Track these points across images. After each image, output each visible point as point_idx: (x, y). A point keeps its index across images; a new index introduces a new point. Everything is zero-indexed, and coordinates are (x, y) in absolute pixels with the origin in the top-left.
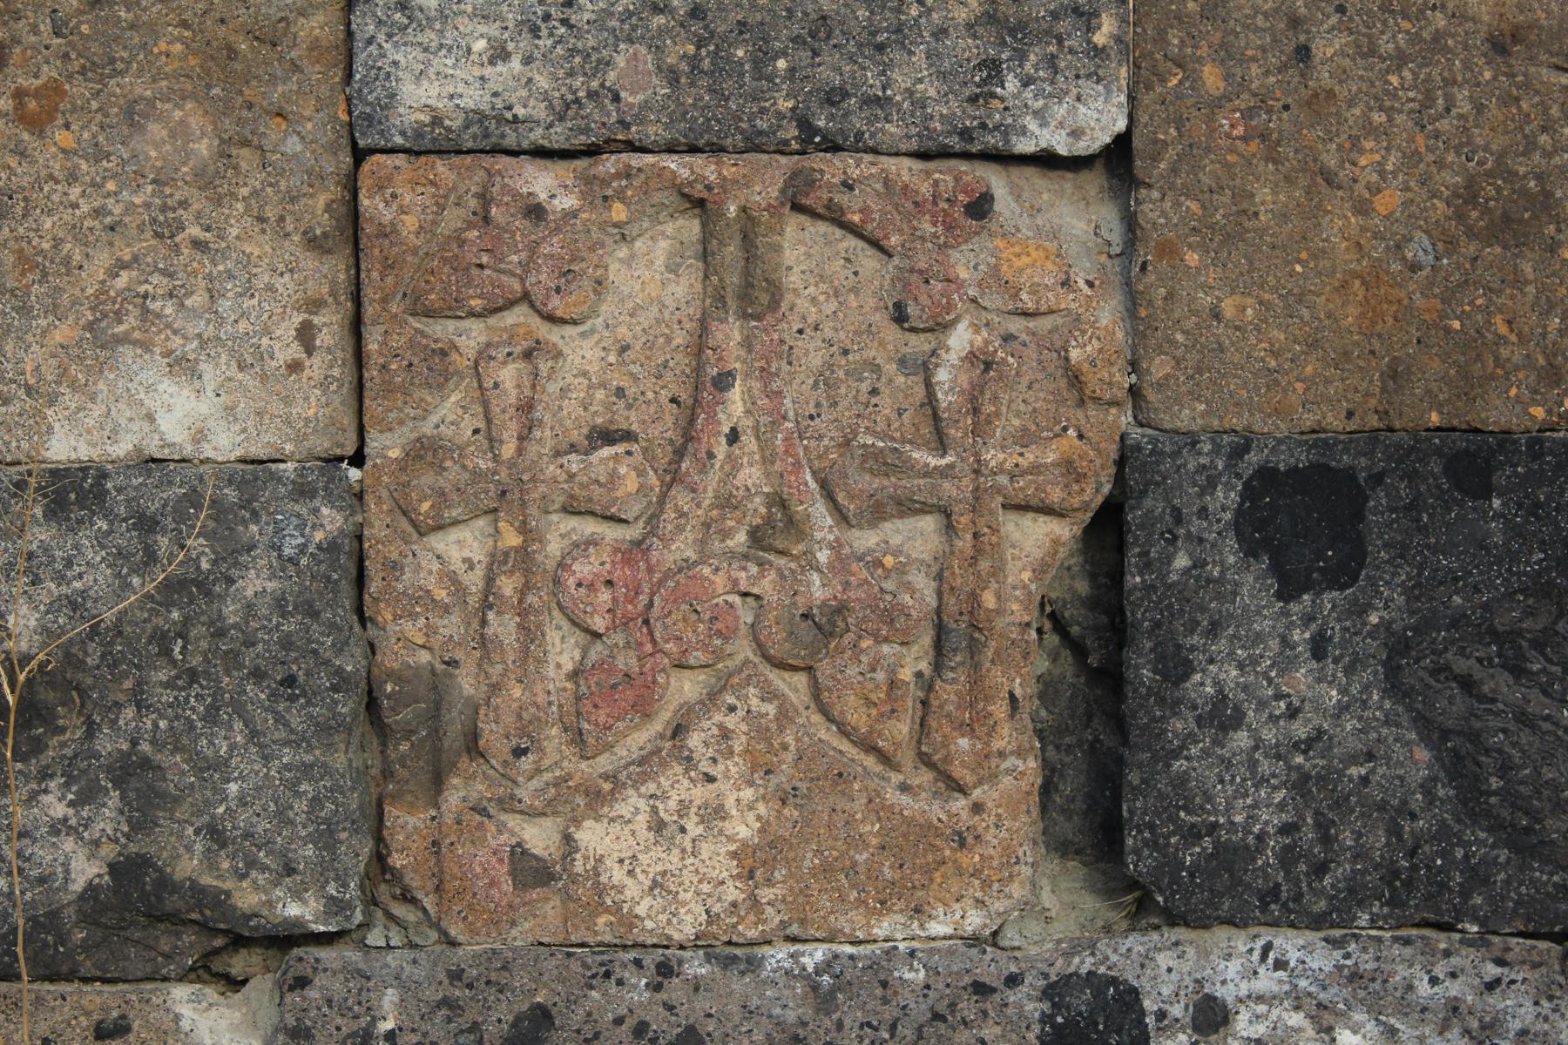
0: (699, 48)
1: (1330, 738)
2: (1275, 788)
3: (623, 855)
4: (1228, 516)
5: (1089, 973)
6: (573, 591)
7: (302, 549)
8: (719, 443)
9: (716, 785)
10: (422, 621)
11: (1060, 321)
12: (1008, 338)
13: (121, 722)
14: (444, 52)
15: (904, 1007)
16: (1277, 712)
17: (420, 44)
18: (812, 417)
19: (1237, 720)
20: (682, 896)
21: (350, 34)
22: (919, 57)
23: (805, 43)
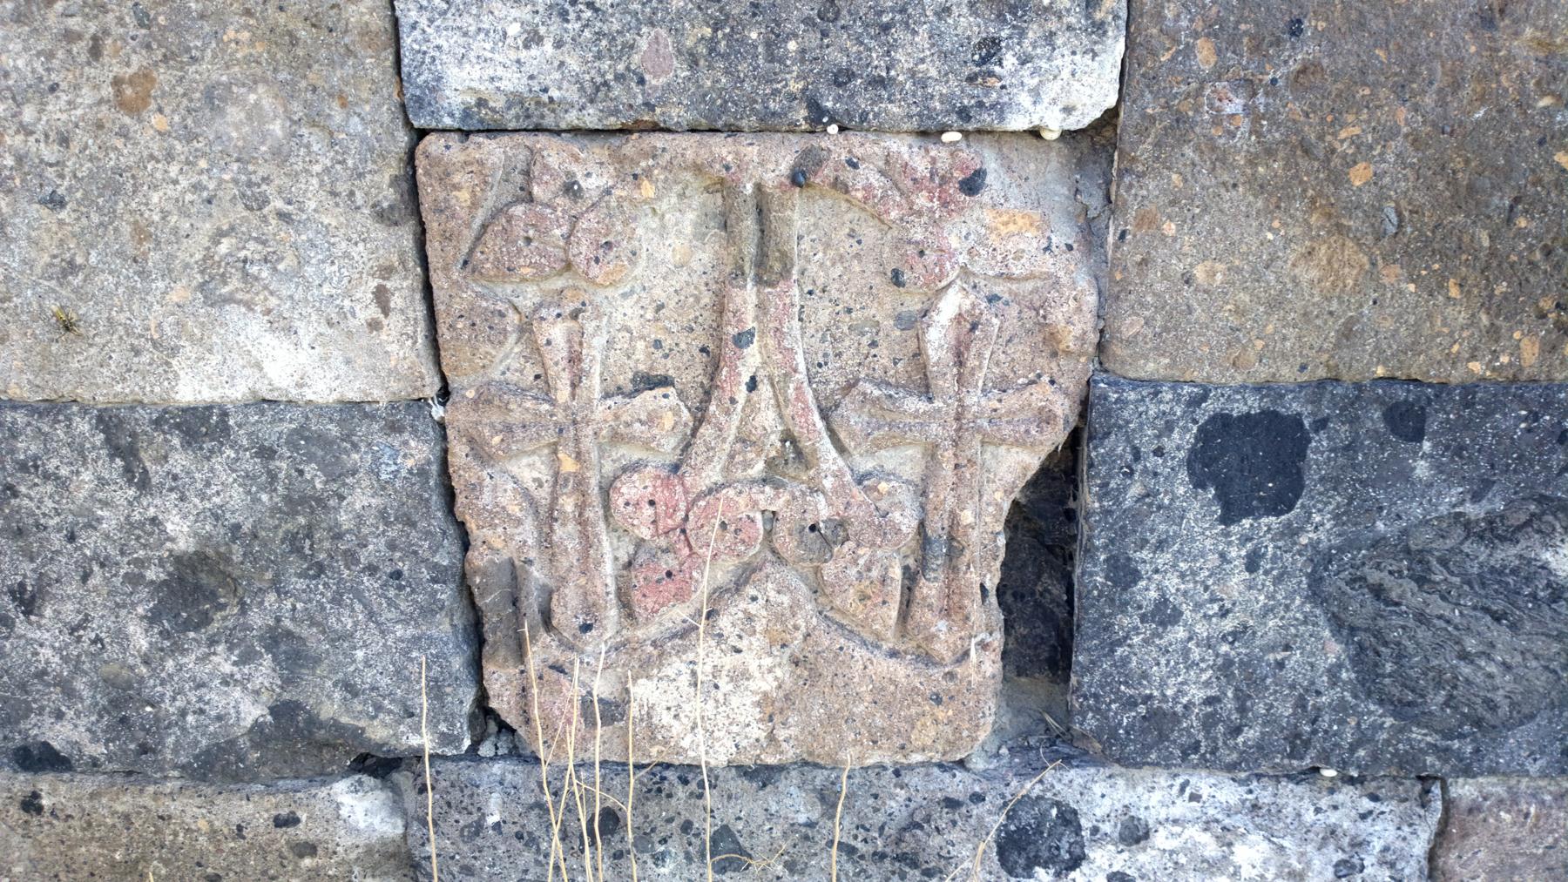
0: (715, 31)
1: (1254, 633)
2: (1203, 670)
4: (1182, 454)
6: (622, 509)
7: (396, 473)
10: (500, 530)
11: (1040, 284)
12: (992, 299)
13: (266, 604)
14: (482, 36)
15: (890, 815)
16: (1211, 613)
17: (460, 28)
18: (820, 365)
19: (1175, 617)
20: (716, 734)
21: (396, 22)
22: (922, 38)
23: (815, 25)
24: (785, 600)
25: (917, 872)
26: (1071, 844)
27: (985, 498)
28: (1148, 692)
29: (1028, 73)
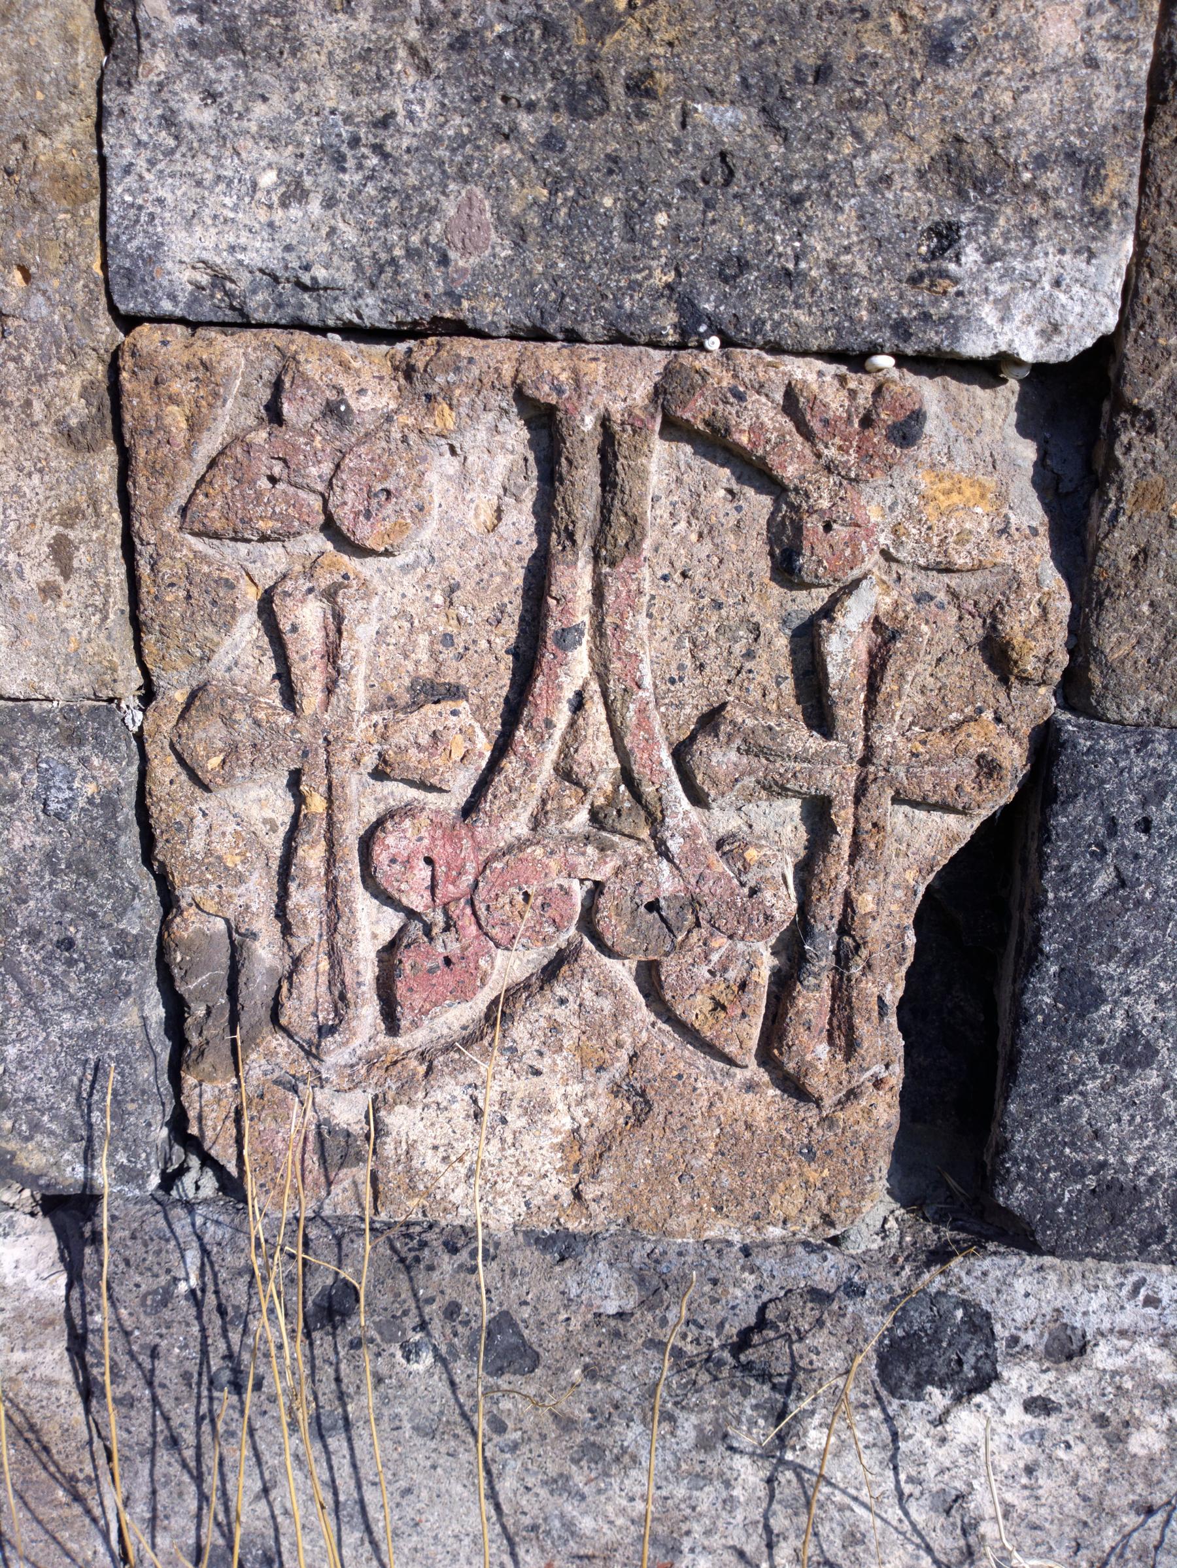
0: (553, 193)
3: (437, 1142)
5: (939, 1293)
6: (386, 868)
7: (70, 802)
8: (560, 711)
9: (541, 1078)
10: (213, 888)
12: (922, 598)
14: (222, 187)
15: (733, 1308)
17: (191, 175)
19: (1149, 1056)
22: (847, 219)
23: (696, 190)
24: (607, 1004)
25: (766, 1388)
26: (979, 1359)
27: (891, 878)
28: (1101, 1158)
29: (996, 275)
